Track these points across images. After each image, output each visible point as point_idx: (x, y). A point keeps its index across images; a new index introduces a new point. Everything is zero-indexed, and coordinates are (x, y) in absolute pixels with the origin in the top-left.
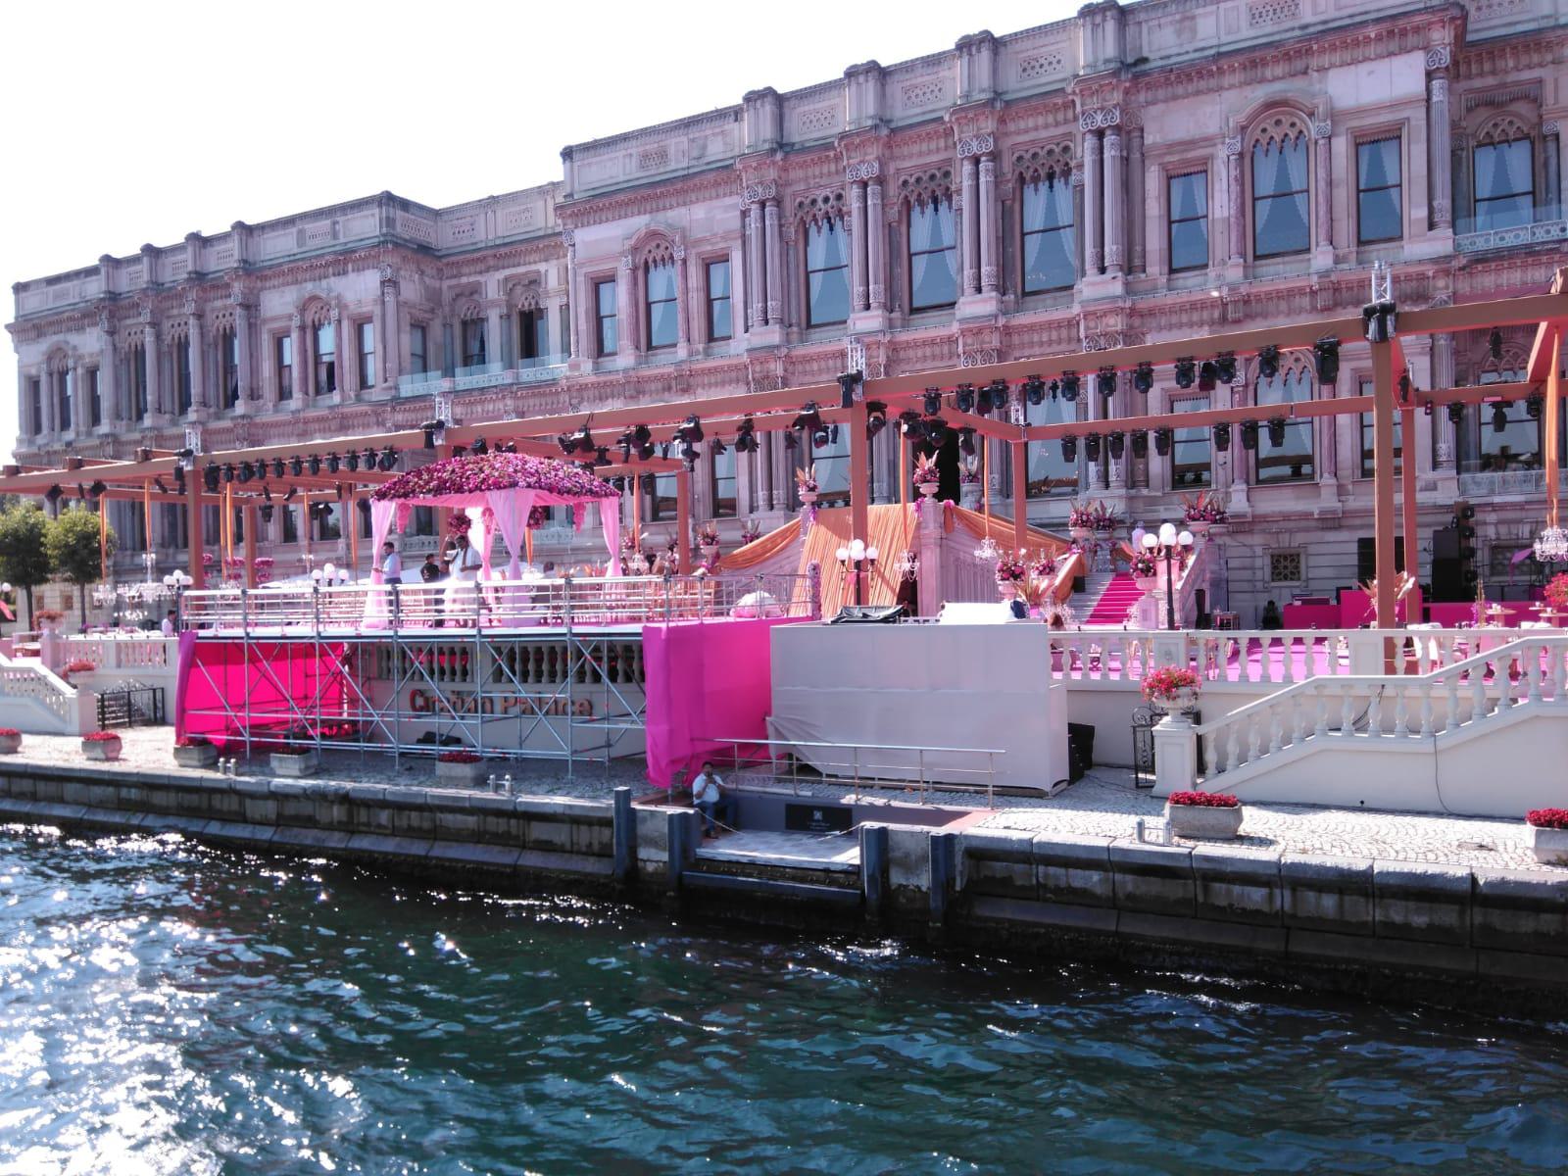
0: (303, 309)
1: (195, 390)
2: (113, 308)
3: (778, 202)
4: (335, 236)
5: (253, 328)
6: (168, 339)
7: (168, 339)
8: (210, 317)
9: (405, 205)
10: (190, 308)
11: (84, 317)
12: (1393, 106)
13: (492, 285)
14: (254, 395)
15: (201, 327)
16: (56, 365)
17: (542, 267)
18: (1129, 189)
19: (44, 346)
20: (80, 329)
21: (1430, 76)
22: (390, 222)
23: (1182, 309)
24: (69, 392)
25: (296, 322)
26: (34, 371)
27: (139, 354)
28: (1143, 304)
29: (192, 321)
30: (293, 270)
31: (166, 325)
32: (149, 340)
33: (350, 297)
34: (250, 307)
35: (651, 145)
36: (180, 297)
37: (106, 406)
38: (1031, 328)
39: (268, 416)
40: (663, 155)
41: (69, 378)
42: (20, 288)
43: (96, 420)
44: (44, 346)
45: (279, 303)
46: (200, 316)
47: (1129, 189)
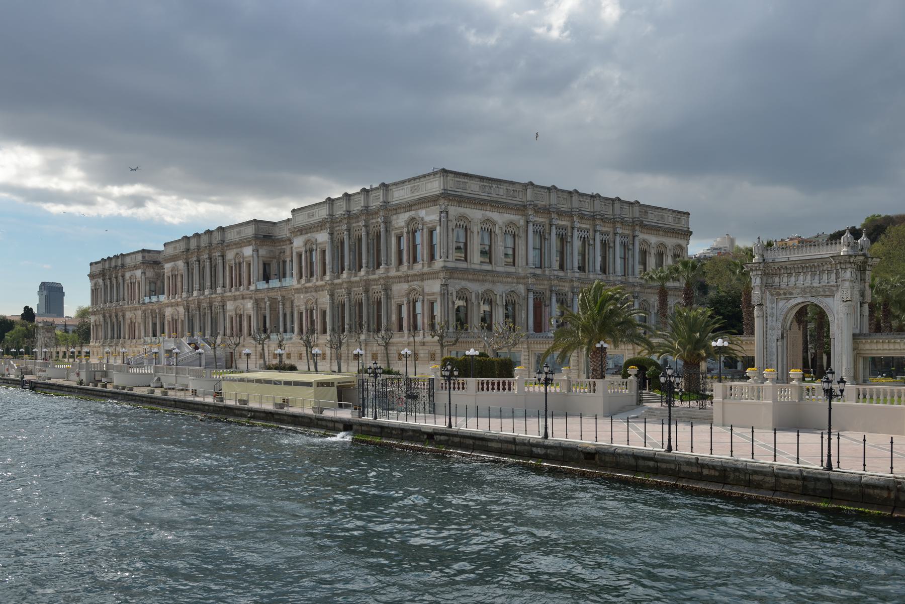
2: (330, 223)
9: (149, 251)
11: (320, 226)
14: (124, 300)
15: (349, 235)
18: (224, 268)
19: (93, 282)
22: (143, 257)
24: (314, 260)
26: (300, 250)
29: (363, 229)
30: (302, 230)
36: (376, 213)
41: (314, 253)
42: (91, 264)
44: (93, 282)
47: (224, 268)
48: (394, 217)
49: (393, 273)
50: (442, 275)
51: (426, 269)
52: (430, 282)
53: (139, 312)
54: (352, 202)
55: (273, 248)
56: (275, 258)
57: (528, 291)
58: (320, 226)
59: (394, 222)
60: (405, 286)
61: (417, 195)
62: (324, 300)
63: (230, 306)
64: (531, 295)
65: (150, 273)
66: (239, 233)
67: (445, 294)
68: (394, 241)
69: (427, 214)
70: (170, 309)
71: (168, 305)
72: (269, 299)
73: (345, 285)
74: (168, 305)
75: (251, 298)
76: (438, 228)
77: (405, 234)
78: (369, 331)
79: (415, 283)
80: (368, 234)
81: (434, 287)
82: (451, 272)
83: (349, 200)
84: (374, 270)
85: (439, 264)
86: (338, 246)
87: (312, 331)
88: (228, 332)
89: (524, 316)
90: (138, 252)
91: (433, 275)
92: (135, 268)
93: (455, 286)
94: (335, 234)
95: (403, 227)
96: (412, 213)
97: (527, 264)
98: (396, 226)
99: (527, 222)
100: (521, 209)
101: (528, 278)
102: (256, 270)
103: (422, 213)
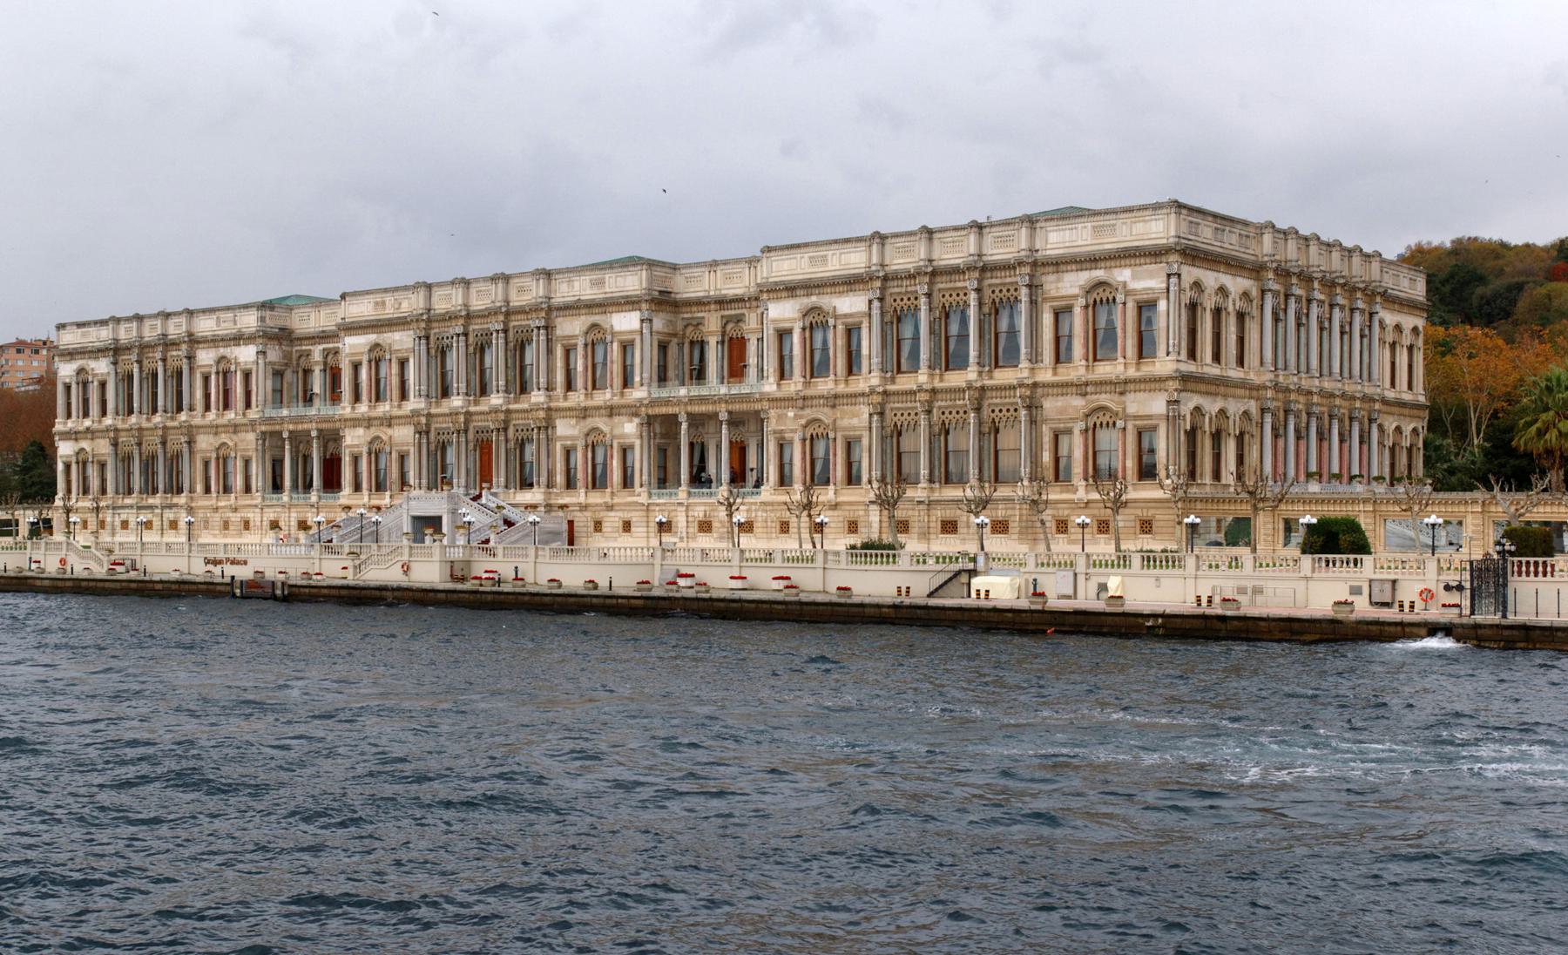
0: (218, 362)
1: (160, 403)
3: (427, 338)
4: (235, 323)
5: (191, 369)
6: (146, 370)
7: (146, 370)
8: (169, 361)
10: (158, 355)
12: (631, 332)
13: (317, 352)
14: (191, 409)
16: (81, 377)
18: (550, 351)
20: (97, 358)
21: (642, 321)
22: (262, 319)
23: (570, 409)
25: (214, 370)
27: (130, 377)
28: (553, 405)
31: (145, 362)
32: (136, 371)
33: (241, 359)
34: (191, 358)
35: (378, 298)
37: (110, 406)
38: (517, 411)
39: (197, 421)
40: (383, 303)
43: (104, 413)
45: (206, 357)
46: (164, 360)
47: (550, 351)
48: (1051, 278)
49: (1045, 376)
50: (1173, 385)
51: (1132, 373)
52: (1140, 396)
53: (251, 437)
54: (936, 243)
55: (669, 317)
56: (675, 335)
57: (1263, 411)
58: (851, 283)
59: (1046, 287)
60: (1078, 403)
61: (1109, 243)
62: (855, 421)
63: (566, 429)
64: (1268, 419)
65: (274, 354)
66: (601, 283)
67: (1172, 419)
68: (1047, 319)
69: (1134, 277)
70: (361, 431)
71: (355, 422)
72: (689, 415)
73: (923, 396)
74: (355, 422)
75: (636, 415)
76: (1162, 305)
77: (1077, 310)
78: (931, 481)
79: (1103, 396)
80: (980, 304)
81: (1157, 405)
82: (1187, 381)
83: (930, 239)
84: (990, 371)
85: (1164, 364)
86: (895, 319)
87: (902, 478)
88: (560, 478)
89: (1255, 454)
90: (246, 307)
91: (1155, 382)
92: (238, 339)
93: (1190, 402)
94: (889, 300)
95: (1075, 297)
96: (1099, 274)
97: (1262, 364)
98: (1053, 293)
99: (1263, 292)
100: (1256, 270)
101: (1266, 388)
102: (644, 360)
103: (1123, 275)
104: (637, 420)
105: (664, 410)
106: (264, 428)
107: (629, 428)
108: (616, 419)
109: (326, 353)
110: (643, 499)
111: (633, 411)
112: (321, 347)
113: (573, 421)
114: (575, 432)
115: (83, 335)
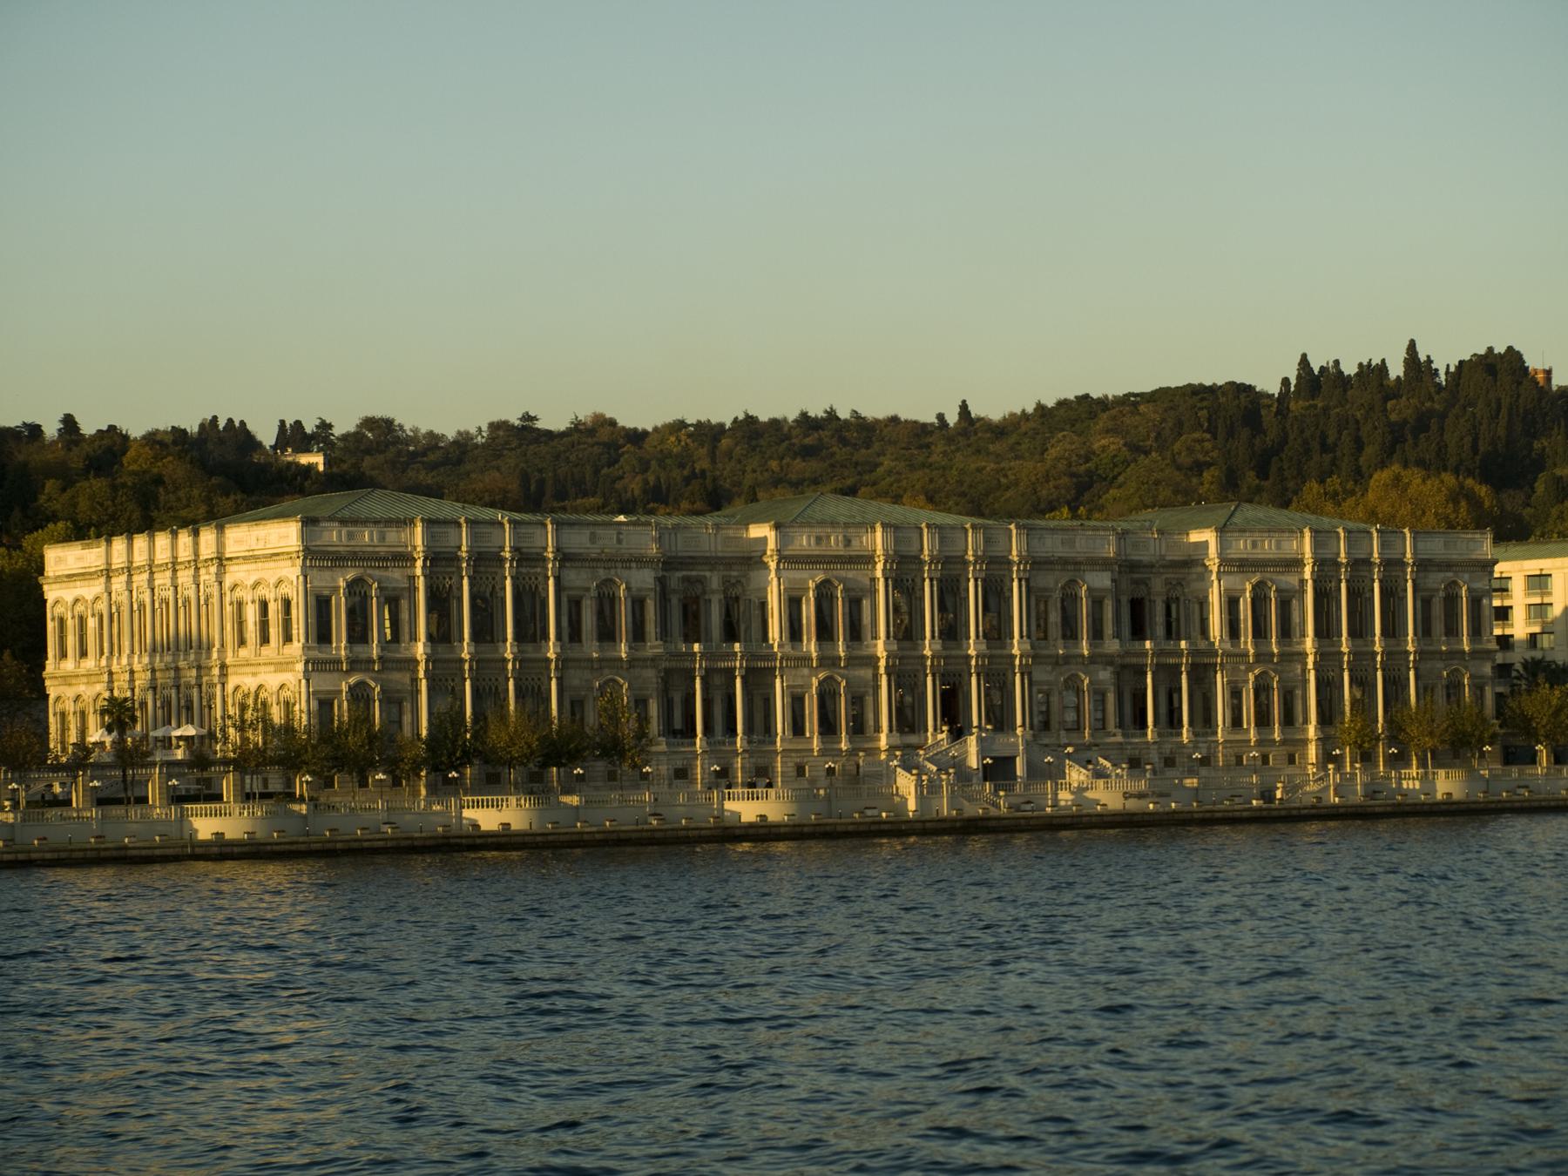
4: (619, 541)
12: (1102, 590)
17: (708, 574)
53: (650, 674)
75: (1111, 663)
104: (1110, 669)
105: (1134, 660)
106: (664, 665)
107: (1105, 675)
108: (1092, 667)
109: (727, 584)
110: (1119, 739)
111: (1108, 660)
112: (679, 574)
113: (1049, 668)
114: (1051, 678)
115: (350, 536)
